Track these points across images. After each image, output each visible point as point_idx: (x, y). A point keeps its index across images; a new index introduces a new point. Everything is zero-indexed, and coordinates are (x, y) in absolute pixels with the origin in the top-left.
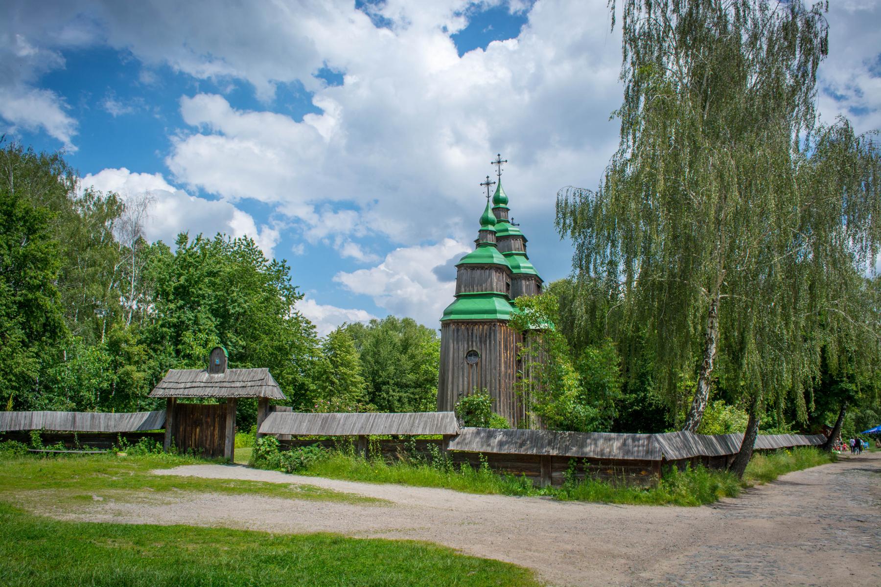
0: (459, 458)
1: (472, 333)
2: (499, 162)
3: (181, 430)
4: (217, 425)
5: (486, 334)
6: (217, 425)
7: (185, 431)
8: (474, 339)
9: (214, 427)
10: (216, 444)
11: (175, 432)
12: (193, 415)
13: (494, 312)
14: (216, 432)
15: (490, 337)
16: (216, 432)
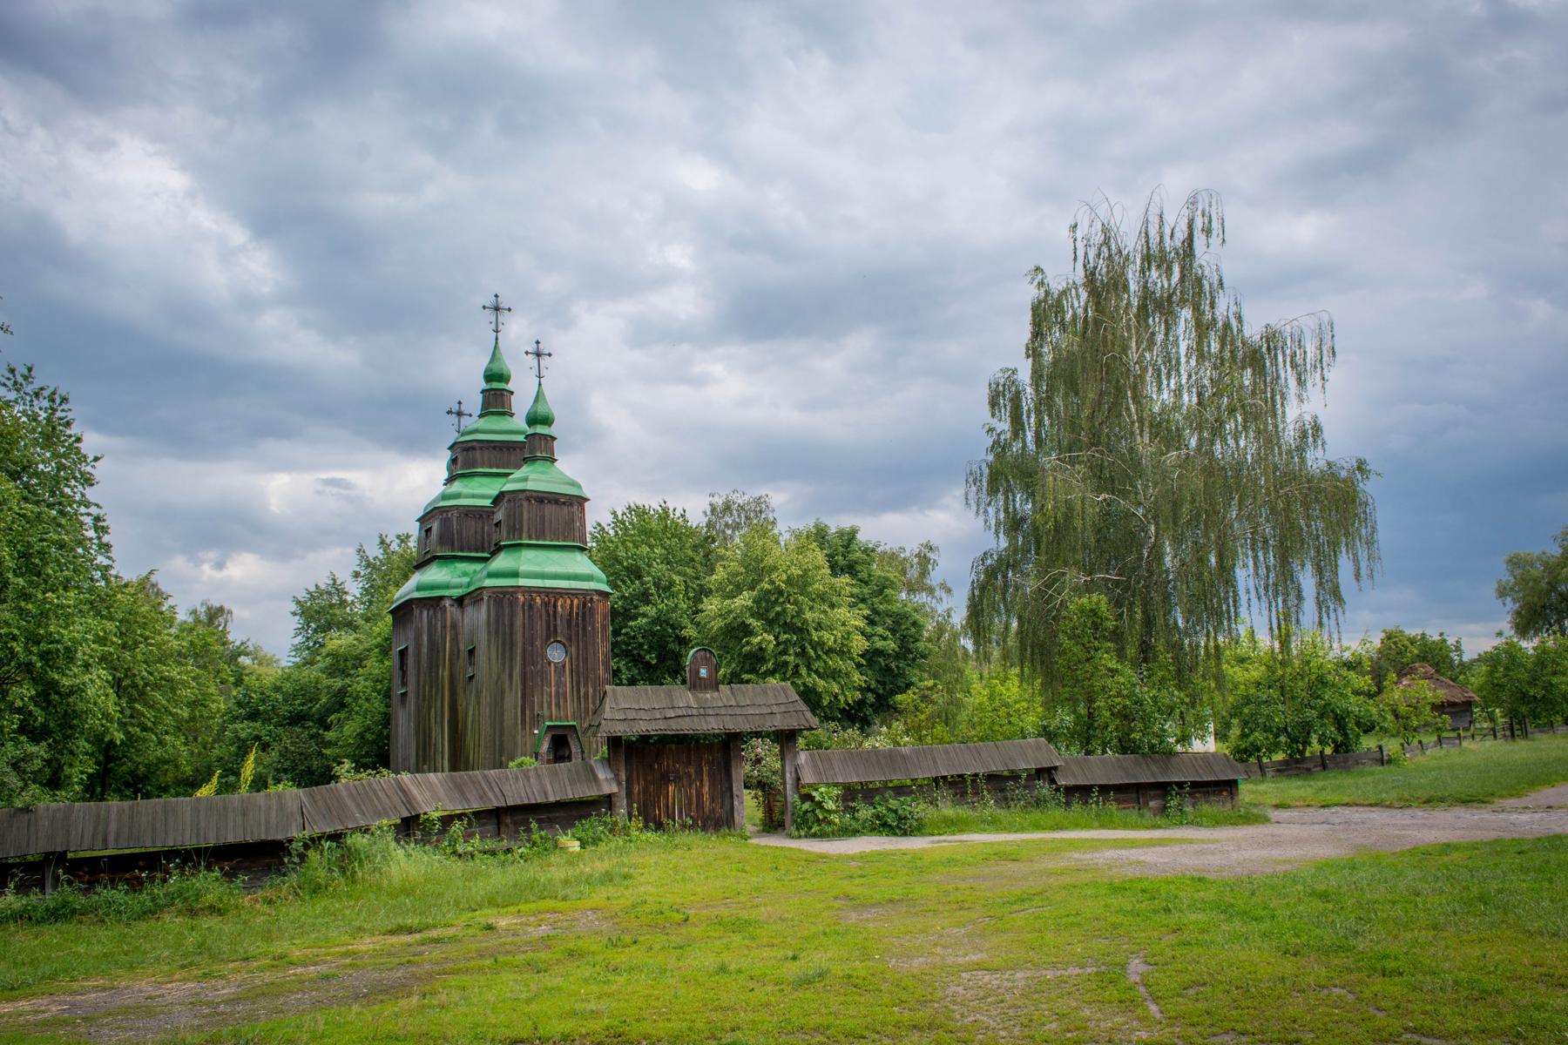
0: (1071, 791)
1: (555, 612)
2: (497, 309)
3: (636, 791)
4: (705, 778)
5: (577, 614)
6: (705, 778)
7: (646, 790)
8: (559, 622)
9: (702, 781)
10: (706, 810)
11: (629, 794)
12: (660, 765)
13: (590, 578)
14: (706, 789)
15: (584, 619)
16: (706, 789)
